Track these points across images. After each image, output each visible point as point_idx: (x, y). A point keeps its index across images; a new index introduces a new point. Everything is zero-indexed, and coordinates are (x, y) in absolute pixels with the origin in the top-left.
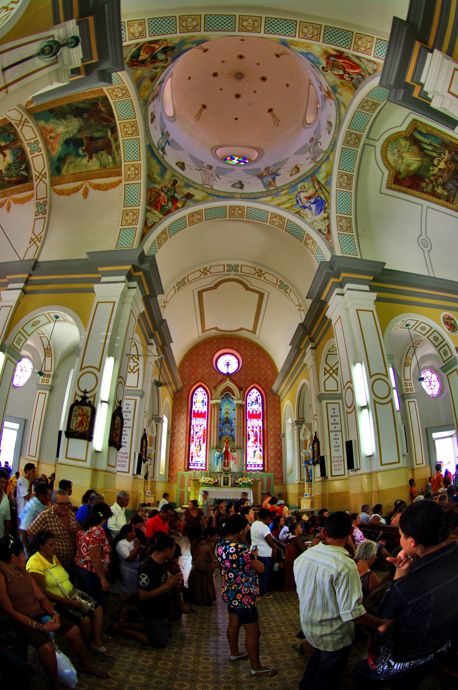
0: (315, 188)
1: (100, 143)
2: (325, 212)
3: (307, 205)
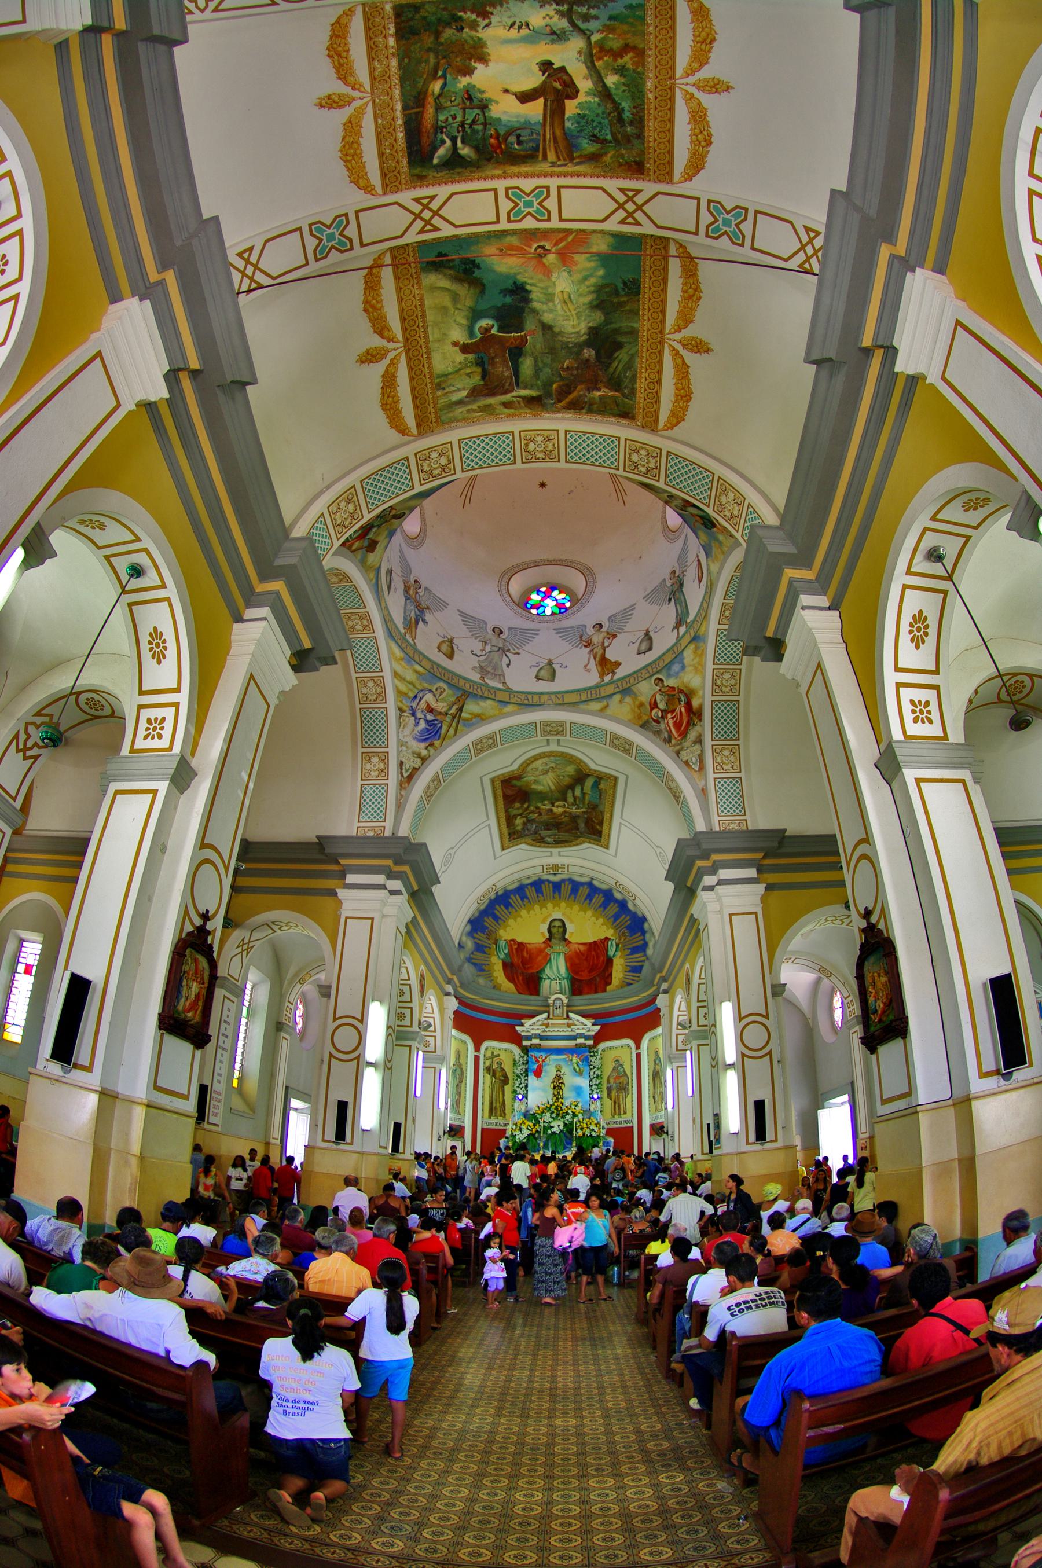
0: (450, 709)
1: (503, 370)
2: (426, 748)
3: (419, 715)
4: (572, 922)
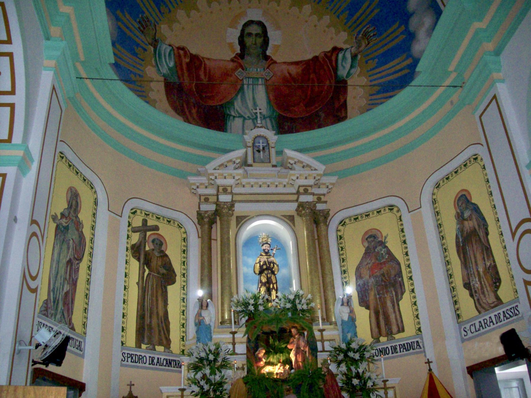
4: (278, 28)
